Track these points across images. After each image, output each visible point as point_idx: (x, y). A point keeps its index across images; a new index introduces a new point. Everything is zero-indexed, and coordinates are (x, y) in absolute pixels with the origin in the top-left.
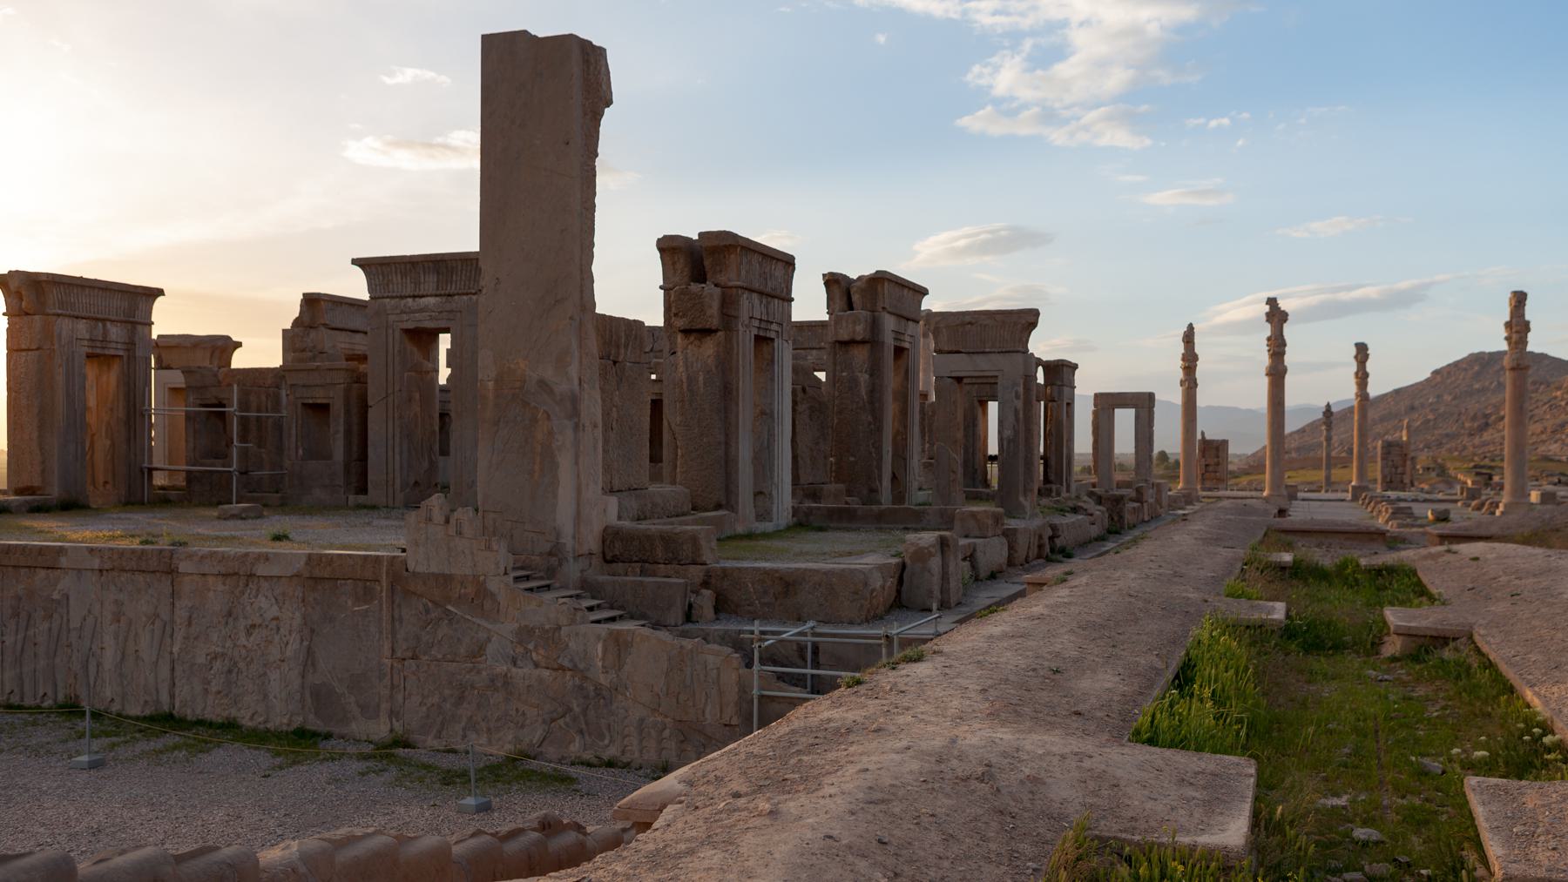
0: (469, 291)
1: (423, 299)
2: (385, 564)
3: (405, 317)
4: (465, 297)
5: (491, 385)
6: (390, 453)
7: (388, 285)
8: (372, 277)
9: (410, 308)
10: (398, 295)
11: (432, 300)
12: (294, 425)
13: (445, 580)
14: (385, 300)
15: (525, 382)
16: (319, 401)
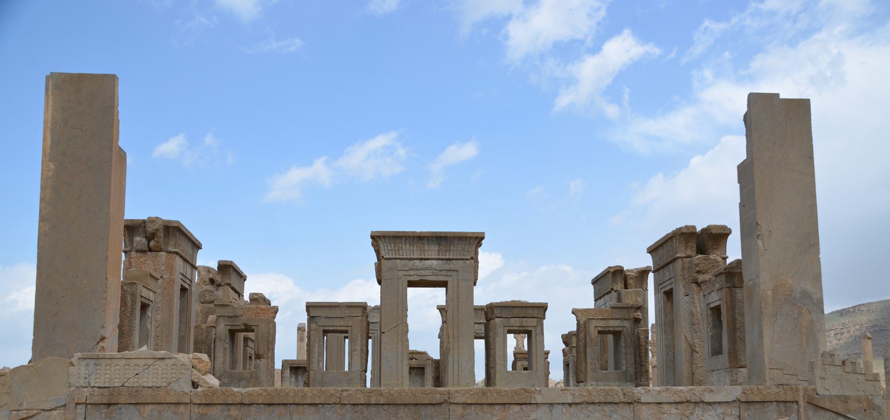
0: (465, 257)
1: (427, 261)
2: (801, 391)
3: (412, 273)
4: (461, 262)
5: (769, 293)
6: (400, 365)
7: (398, 251)
8: (385, 244)
9: (417, 266)
10: (409, 257)
11: (434, 262)
12: (318, 344)
13: (845, 399)
14: (396, 260)
15: (793, 291)
16: (338, 328)
